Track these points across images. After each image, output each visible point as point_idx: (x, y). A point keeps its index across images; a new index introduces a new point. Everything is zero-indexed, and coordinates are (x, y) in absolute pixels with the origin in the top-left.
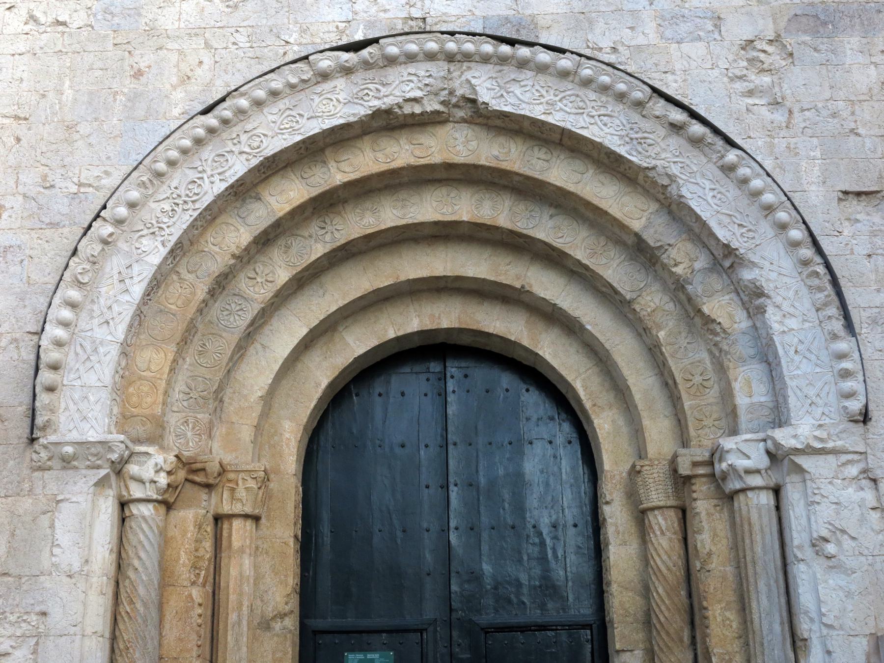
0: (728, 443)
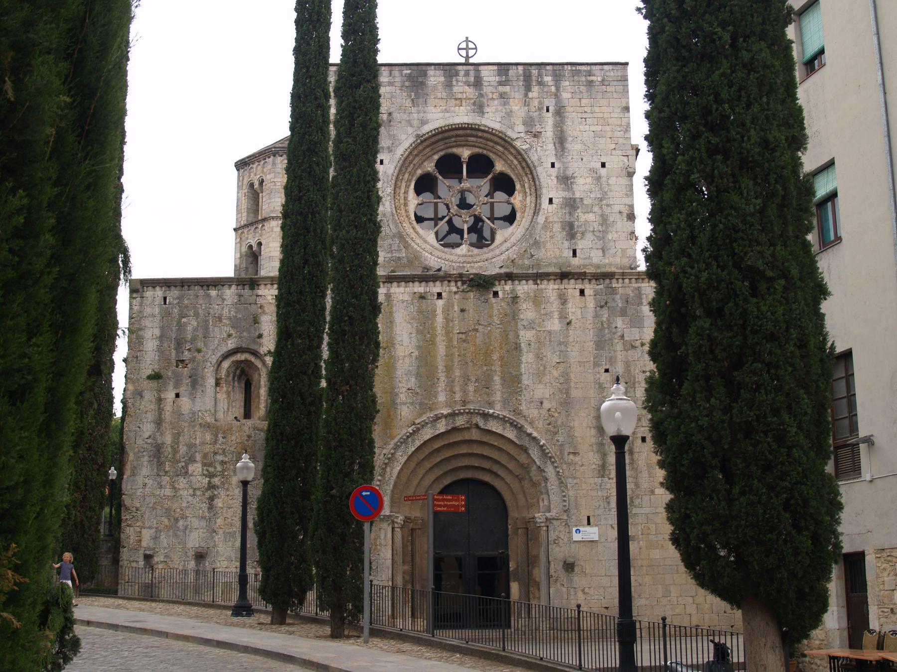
0: (536, 515)
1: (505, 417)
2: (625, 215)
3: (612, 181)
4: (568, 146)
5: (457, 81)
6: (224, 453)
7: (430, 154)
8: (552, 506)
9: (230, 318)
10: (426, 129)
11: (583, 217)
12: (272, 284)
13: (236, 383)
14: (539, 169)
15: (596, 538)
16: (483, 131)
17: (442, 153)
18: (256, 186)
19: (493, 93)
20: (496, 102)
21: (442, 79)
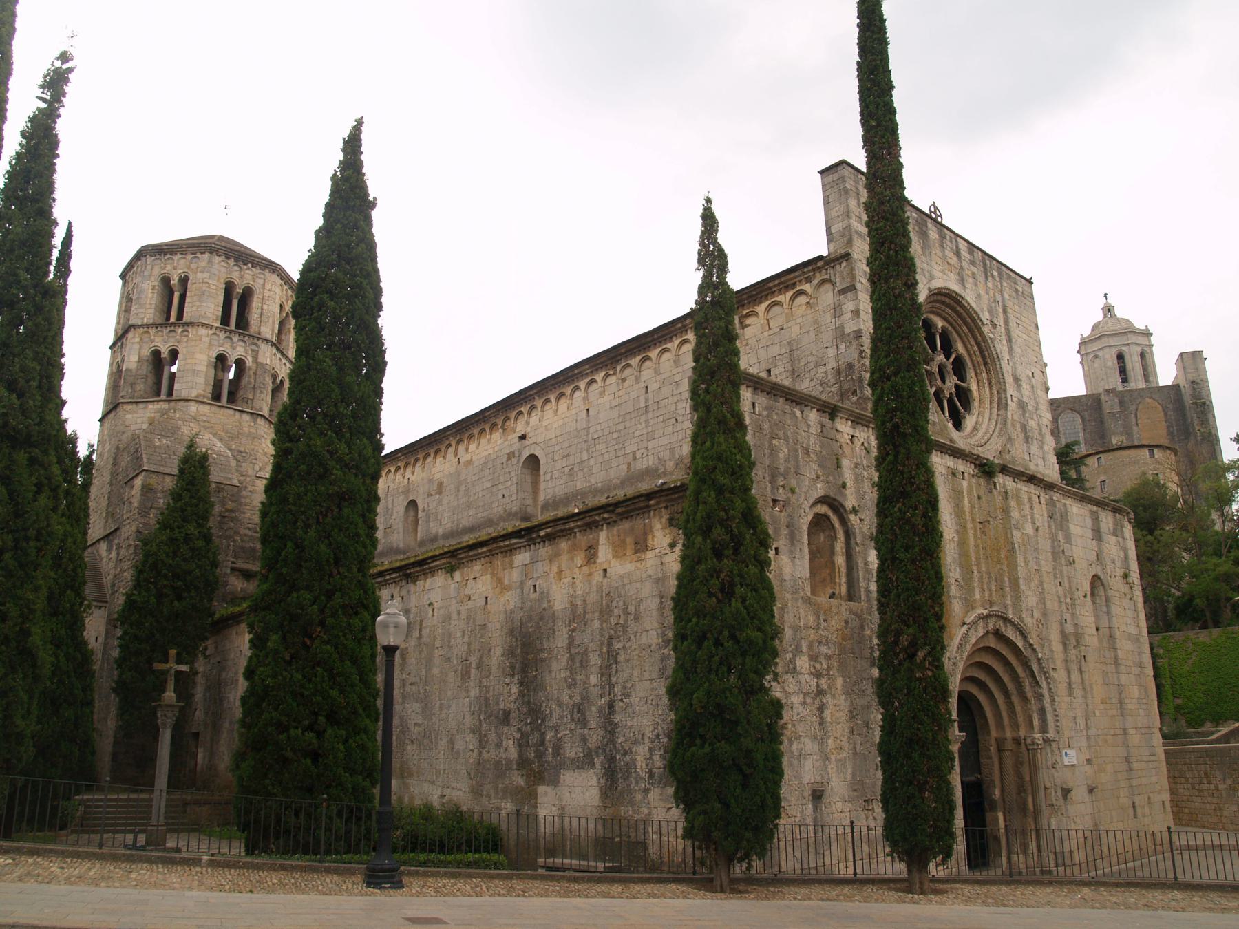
16: (962, 306)
18: (175, 281)
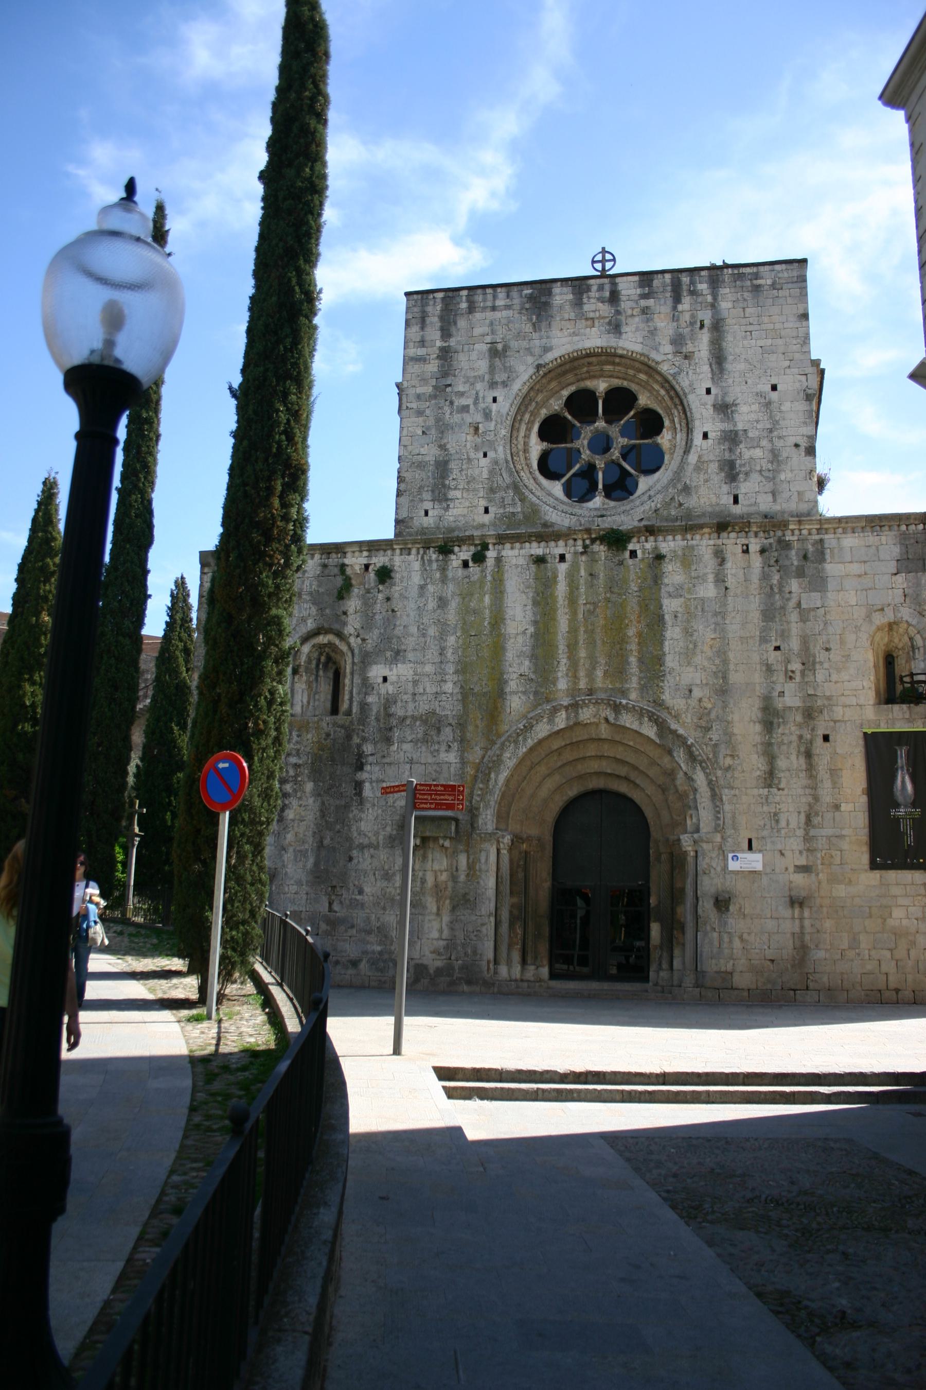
0: (681, 837)
1: (642, 709)
2: (802, 449)
3: (786, 406)
4: (728, 366)
5: (589, 298)
6: (298, 753)
7: (557, 389)
8: (701, 825)
9: (311, 593)
10: (550, 356)
11: (747, 454)
12: (361, 551)
13: (321, 673)
14: (691, 398)
15: (759, 867)
16: (621, 356)
17: (573, 388)
19: (633, 309)
20: (637, 319)
21: (571, 297)
